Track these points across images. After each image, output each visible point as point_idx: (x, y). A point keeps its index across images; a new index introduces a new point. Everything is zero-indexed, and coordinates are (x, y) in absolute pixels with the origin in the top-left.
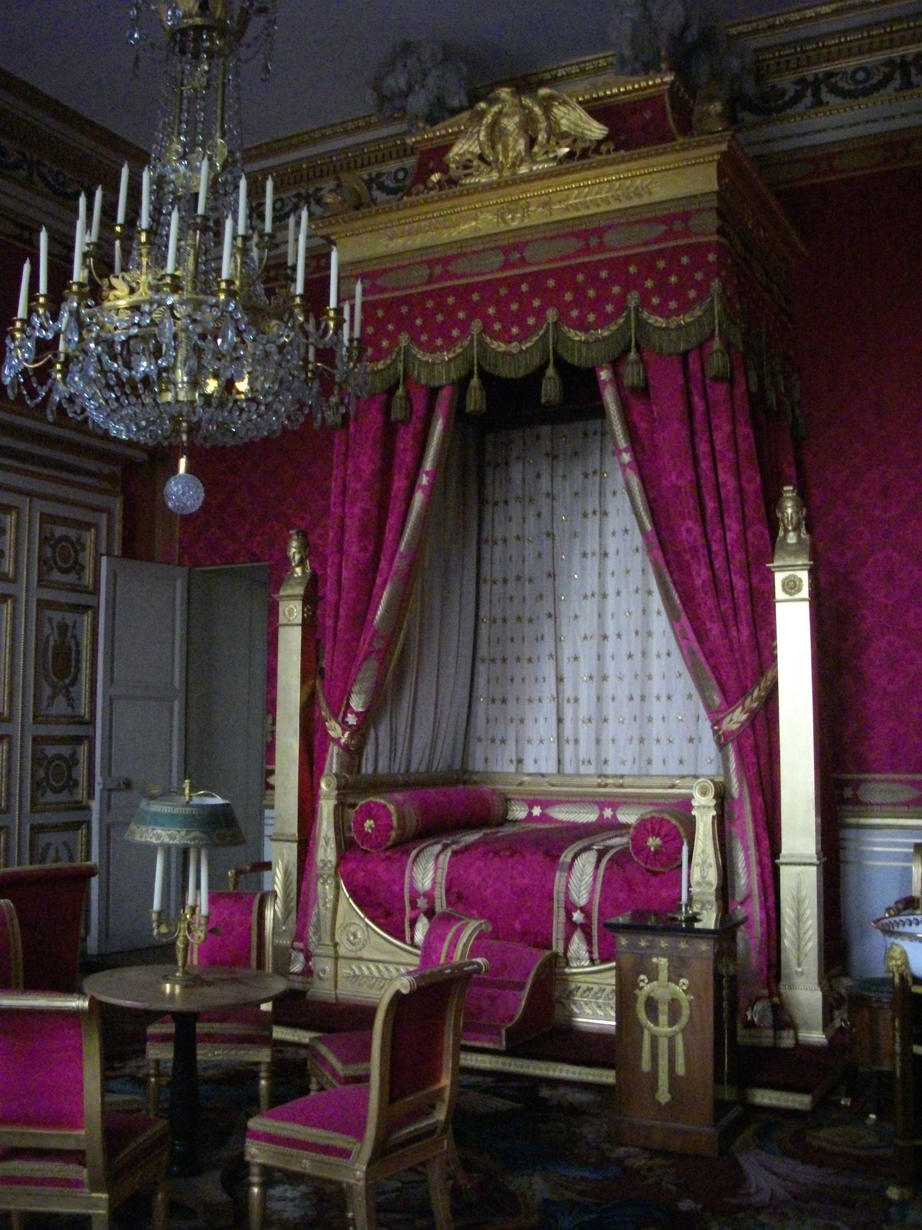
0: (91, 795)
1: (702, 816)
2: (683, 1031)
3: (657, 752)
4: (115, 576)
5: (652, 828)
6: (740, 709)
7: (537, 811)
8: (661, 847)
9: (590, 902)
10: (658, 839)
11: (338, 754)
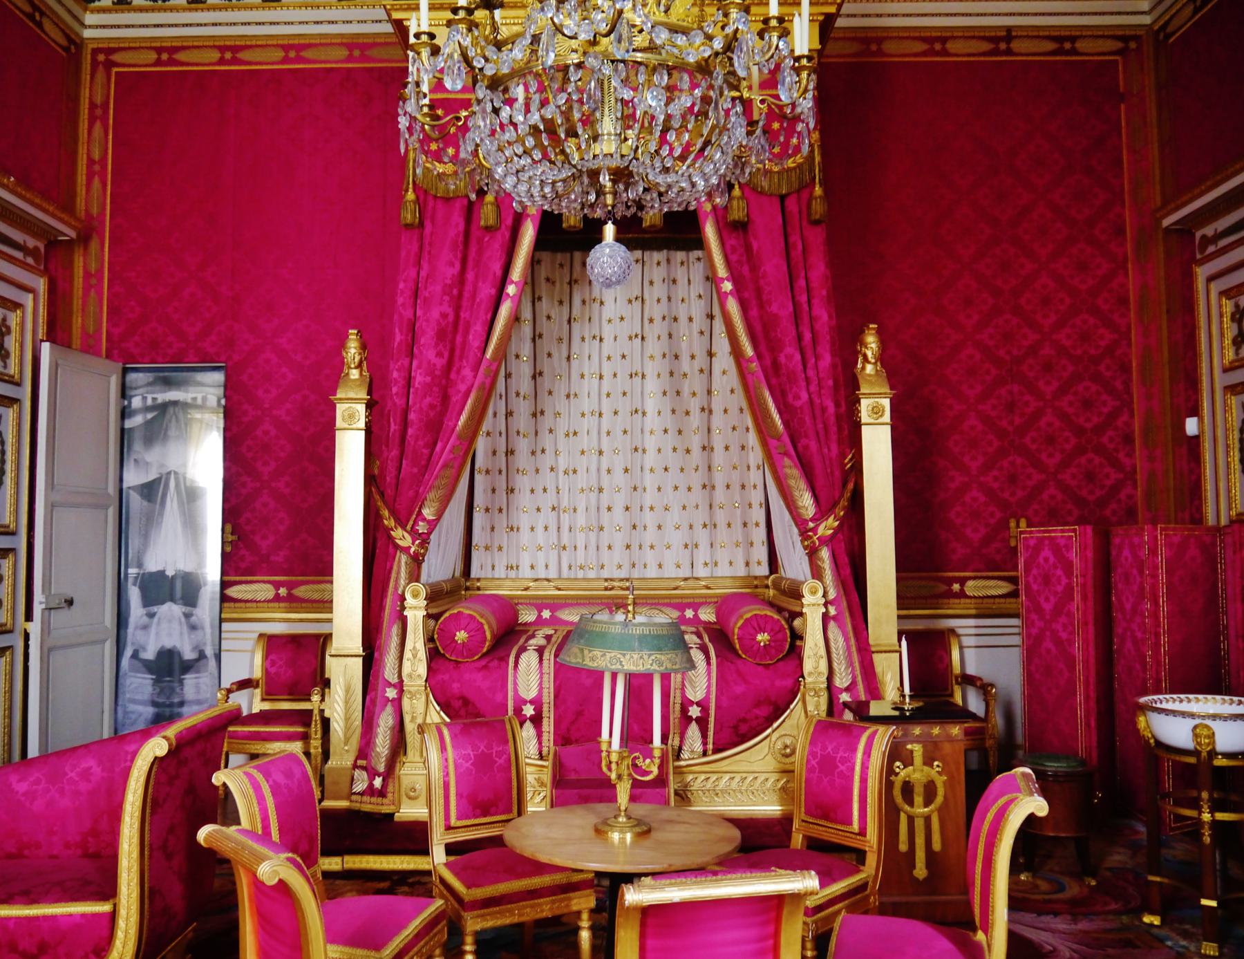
0: (29, 617)
1: (812, 612)
2: (940, 810)
3: (650, 557)
4: (57, 365)
5: (759, 625)
6: (833, 516)
7: (546, 614)
8: (769, 641)
9: (707, 698)
10: (766, 634)
11: (406, 563)
